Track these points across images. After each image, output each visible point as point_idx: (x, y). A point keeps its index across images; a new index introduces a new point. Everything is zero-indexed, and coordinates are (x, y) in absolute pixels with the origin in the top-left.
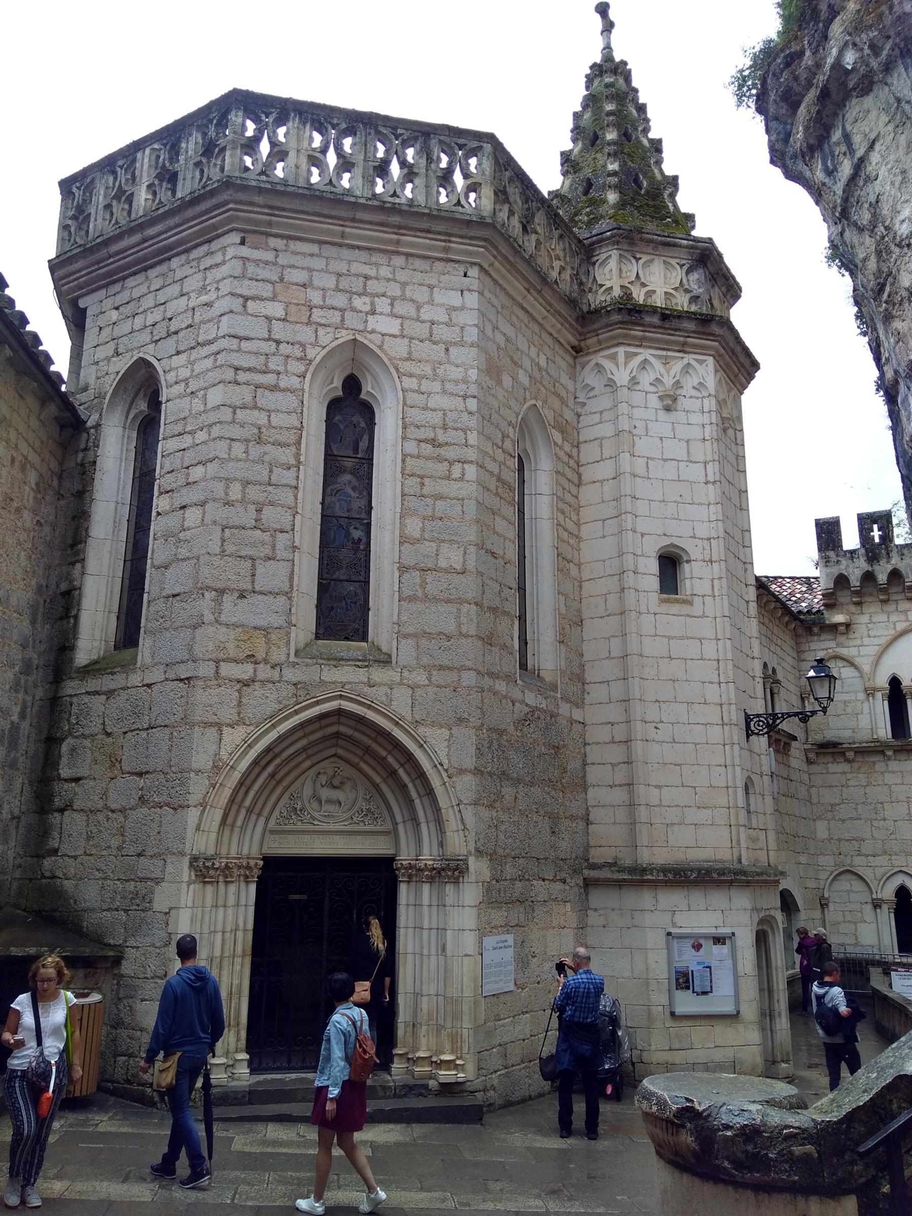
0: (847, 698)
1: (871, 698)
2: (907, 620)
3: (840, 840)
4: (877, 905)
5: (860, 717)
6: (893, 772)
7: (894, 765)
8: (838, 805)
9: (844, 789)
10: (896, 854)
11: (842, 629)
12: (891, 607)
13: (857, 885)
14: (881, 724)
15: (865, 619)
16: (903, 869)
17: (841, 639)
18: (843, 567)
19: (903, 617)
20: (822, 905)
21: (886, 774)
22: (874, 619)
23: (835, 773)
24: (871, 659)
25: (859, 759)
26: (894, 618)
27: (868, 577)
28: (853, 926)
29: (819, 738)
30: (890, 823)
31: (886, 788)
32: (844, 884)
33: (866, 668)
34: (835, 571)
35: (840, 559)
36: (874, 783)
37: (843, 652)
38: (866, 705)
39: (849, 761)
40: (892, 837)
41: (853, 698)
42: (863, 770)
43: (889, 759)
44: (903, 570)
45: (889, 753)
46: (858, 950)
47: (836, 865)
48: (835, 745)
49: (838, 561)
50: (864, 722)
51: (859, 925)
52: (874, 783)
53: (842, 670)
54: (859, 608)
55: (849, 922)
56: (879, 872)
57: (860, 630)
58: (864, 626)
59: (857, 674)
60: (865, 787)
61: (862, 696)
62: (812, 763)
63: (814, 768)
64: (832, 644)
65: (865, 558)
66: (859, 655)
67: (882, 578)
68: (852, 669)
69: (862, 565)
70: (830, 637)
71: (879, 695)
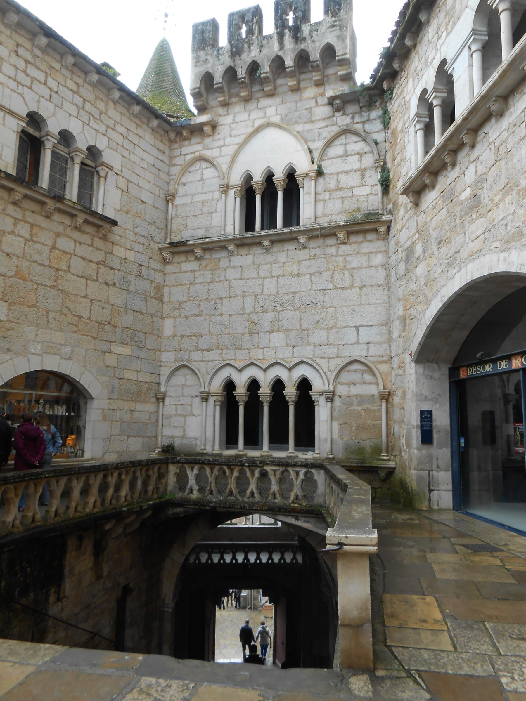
0: (206, 198)
1: (224, 195)
2: (264, 117)
3: (182, 336)
4: (205, 398)
5: (214, 215)
6: (235, 267)
7: (236, 260)
8: (185, 302)
9: (191, 286)
10: (227, 348)
11: (207, 129)
12: (252, 105)
13: (190, 380)
14: (230, 221)
15: (229, 119)
16: (230, 362)
17: (207, 141)
18: (209, 65)
19: (260, 114)
20: (158, 399)
21: (228, 270)
22: (238, 119)
23: (185, 272)
24: (229, 158)
25: (207, 256)
26: (254, 115)
27: (231, 73)
28: (182, 419)
29: (176, 238)
30: (226, 318)
31: (227, 283)
32: (179, 379)
33: (225, 167)
34: (203, 69)
35: (208, 57)
36: (217, 279)
37: (208, 153)
38: (219, 203)
39: (197, 259)
40: (226, 331)
41: (210, 198)
42: (209, 267)
43: (232, 253)
44: (259, 61)
45: (231, 247)
46: (185, 441)
47: (176, 361)
48: (183, 244)
49: (206, 60)
50: (217, 220)
51: (187, 418)
52: (217, 279)
53: (205, 172)
54: (225, 109)
55: (180, 415)
56: (211, 365)
57: (223, 131)
58: (228, 127)
59: (216, 174)
60: (209, 283)
61: (217, 195)
62: (168, 263)
63: (169, 268)
64: (199, 147)
65: (230, 54)
66: (221, 156)
67: (241, 72)
68: (213, 170)
69: (227, 61)
70: (199, 140)
71: (232, 193)
